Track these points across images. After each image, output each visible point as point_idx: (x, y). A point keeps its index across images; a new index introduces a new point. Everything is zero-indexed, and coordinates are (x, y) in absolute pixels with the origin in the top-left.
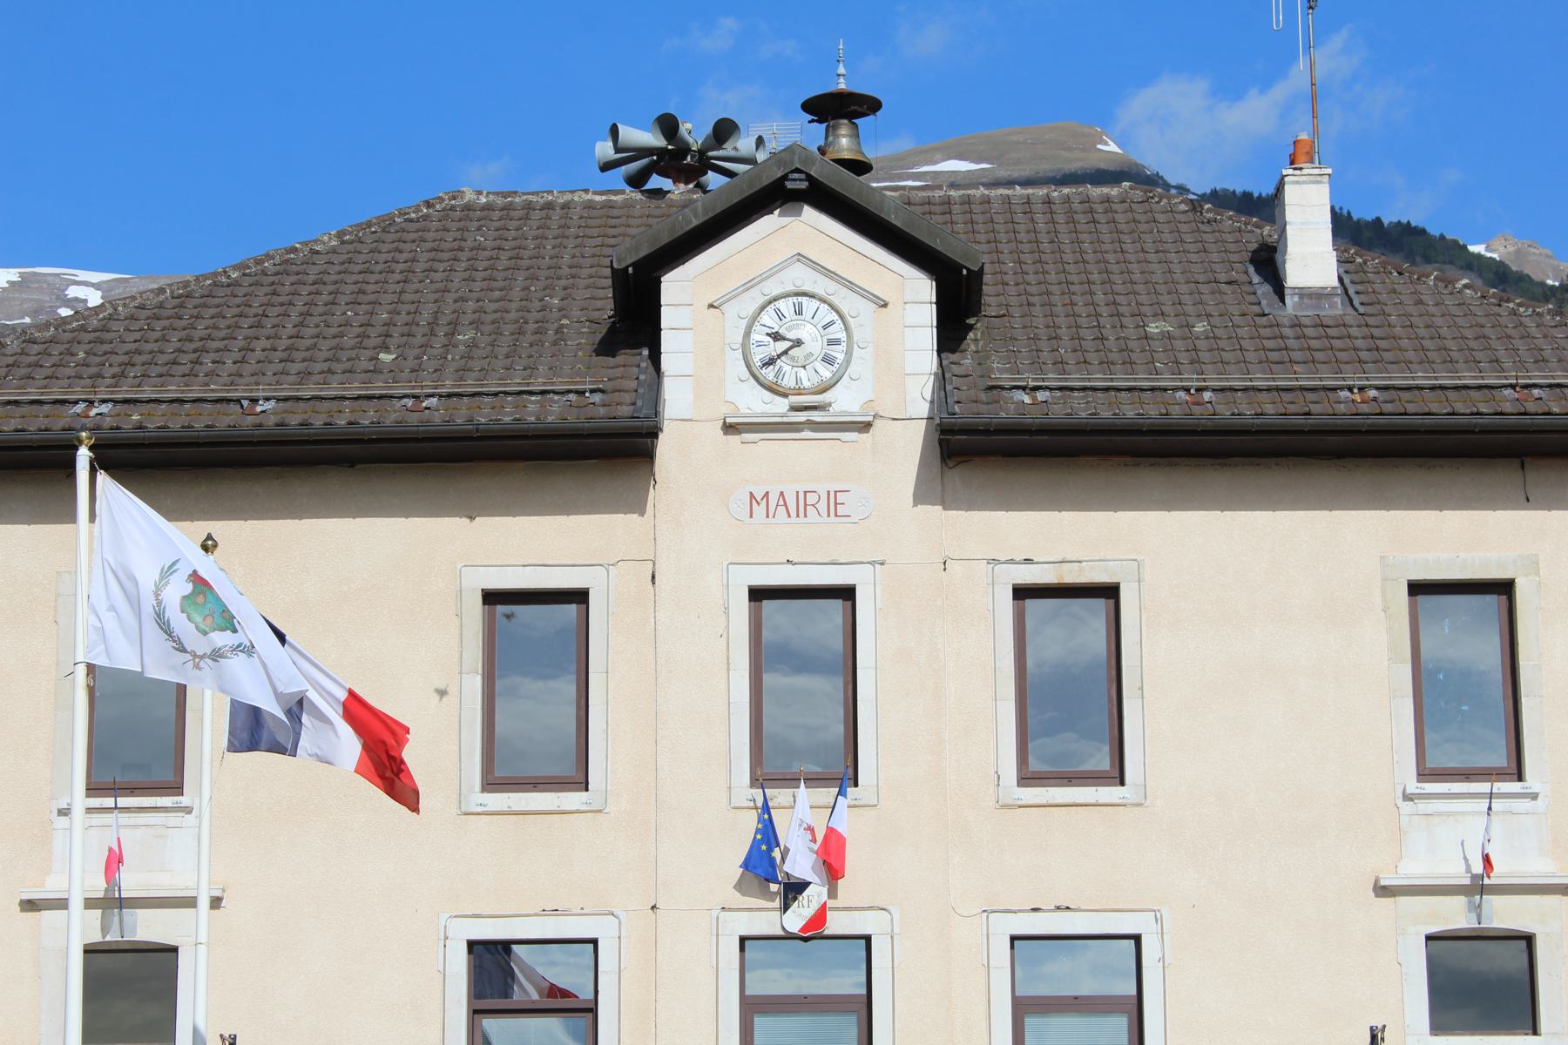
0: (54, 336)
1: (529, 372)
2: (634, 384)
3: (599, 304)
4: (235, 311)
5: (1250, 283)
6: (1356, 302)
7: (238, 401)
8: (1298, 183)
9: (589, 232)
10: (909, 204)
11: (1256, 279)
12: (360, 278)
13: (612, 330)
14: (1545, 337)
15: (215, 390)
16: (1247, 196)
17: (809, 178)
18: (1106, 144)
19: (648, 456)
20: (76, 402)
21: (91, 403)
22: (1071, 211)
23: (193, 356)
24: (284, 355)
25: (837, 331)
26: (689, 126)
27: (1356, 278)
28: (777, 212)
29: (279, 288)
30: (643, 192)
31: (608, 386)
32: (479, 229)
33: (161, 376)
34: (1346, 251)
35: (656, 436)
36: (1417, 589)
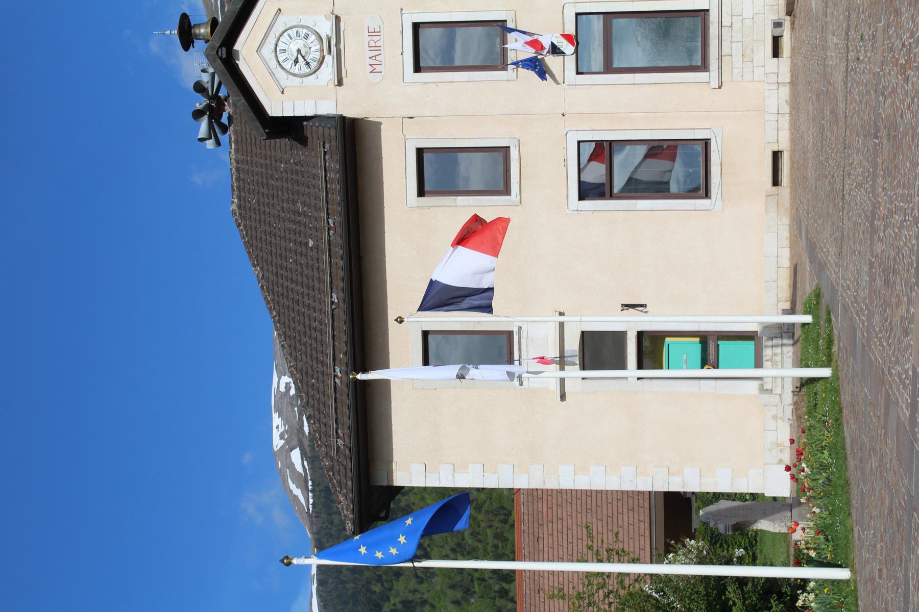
0: (305, 393)
1: (316, 177)
2: (320, 128)
3: (283, 145)
4: (291, 312)
7: (333, 310)
12: (274, 256)
13: (295, 139)
15: (328, 320)
17: (220, 47)
20: (335, 383)
21: (335, 376)
23: (313, 331)
25: (293, 32)
26: (197, 105)
28: (237, 62)
30: (229, 127)
31: (321, 140)
32: (249, 202)
33: (322, 345)
35: (344, 118)
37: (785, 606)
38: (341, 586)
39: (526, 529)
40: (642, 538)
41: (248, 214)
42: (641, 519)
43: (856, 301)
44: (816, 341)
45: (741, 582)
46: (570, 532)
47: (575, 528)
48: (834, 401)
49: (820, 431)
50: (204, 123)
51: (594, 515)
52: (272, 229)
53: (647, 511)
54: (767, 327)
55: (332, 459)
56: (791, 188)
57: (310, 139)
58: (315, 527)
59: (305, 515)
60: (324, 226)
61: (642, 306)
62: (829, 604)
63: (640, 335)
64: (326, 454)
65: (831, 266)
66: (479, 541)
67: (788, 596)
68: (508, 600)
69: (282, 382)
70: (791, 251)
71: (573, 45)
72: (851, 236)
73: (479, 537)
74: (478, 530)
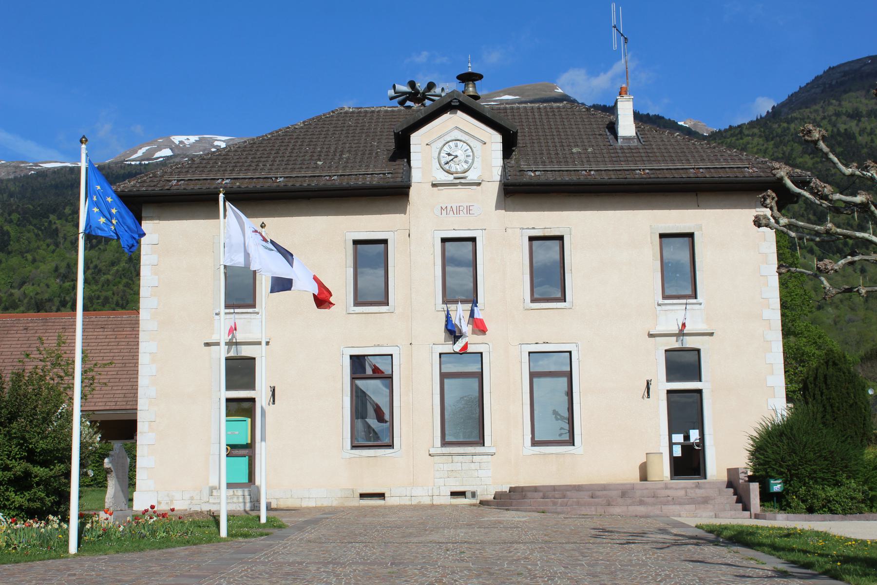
4: (270, 148)
5: (606, 135)
6: (642, 141)
7: (271, 178)
11: (608, 134)
12: (310, 136)
13: (394, 153)
16: (605, 106)
17: (459, 101)
20: (218, 179)
21: (223, 179)
22: (546, 112)
25: (469, 152)
26: (419, 84)
27: (642, 133)
31: (394, 172)
32: (350, 120)
33: (245, 170)
36: (662, 236)
39: (110, 319)
40: (104, 404)
41: (341, 119)
42: (118, 403)
44: (247, 526)
45: (68, 475)
46: (108, 351)
48: (202, 539)
49: (180, 530)
51: (121, 369)
53: (123, 407)
54: (258, 490)
55: (162, 176)
56: (359, 507)
57: (394, 163)
58: (114, 165)
59: (122, 158)
61: (274, 401)
64: (166, 172)
65: (301, 535)
66: (103, 286)
67: (58, 509)
68: (58, 306)
69: (221, 142)
70: (313, 507)
71: (460, 351)
73: (106, 285)
74: (111, 285)
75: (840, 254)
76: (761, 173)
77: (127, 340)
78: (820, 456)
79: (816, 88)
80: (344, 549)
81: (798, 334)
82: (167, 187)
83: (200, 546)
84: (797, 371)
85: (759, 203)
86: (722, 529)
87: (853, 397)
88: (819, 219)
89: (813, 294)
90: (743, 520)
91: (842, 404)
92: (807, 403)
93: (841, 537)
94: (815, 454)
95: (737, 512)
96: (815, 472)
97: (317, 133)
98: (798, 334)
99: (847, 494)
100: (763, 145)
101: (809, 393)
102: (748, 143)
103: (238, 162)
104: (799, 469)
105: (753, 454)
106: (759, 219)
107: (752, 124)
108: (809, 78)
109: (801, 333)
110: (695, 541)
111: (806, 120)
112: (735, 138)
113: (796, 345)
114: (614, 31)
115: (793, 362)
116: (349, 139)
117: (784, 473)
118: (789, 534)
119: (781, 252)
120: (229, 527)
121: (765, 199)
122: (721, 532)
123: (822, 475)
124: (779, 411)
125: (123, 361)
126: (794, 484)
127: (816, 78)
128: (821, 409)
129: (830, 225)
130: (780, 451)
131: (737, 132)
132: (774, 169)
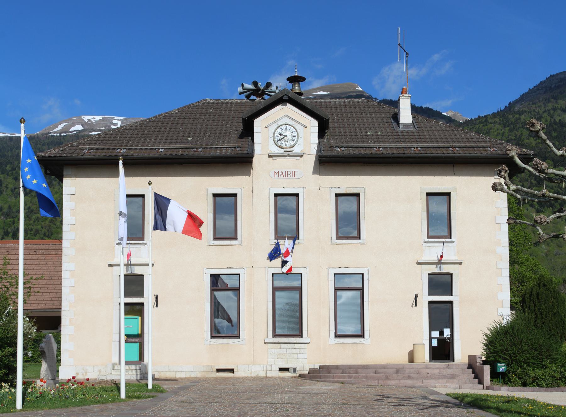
0: (112, 133)
1: (223, 143)
2: (247, 146)
3: (239, 126)
4: (154, 127)
5: (392, 122)
6: (416, 127)
7: (155, 149)
8: (403, 98)
9: (237, 109)
10: (312, 103)
11: (393, 121)
12: (183, 120)
13: (242, 133)
14: (460, 136)
15: (150, 146)
16: (391, 100)
17: (289, 97)
18: (358, 88)
19: (251, 163)
20: (118, 149)
21: (121, 149)
22: (350, 105)
23: (144, 138)
24: (166, 138)
25: (295, 133)
26: (260, 84)
27: (416, 121)
28: (281, 105)
29: (164, 122)
30: (250, 100)
31: (242, 146)
32: (211, 108)
33: (137, 143)
34: (414, 115)
35: (253, 158)
36: (428, 194)
37: (1, 377)
38: (9, 149)
39: (41, 246)
40: (37, 305)
41: (205, 107)
42: (47, 305)
43: (159, 410)
44: (139, 391)
45: (14, 355)
46: (40, 268)
47: (42, 271)
48: (108, 400)
49: (93, 393)
50: (251, 87)
51: (48, 281)
52: (197, 119)
53: (51, 307)
54: (146, 367)
55: (78, 146)
56: (216, 378)
57: (242, 140)
58: (41, 136)
59: (47, 131)
60: (198, 146)
61: (157, 305)
62: (3, 399)
63: (142, 304)
64: (80, 143)
65: (177, 398)
66: (34, 221)
67: (7, 378)
68: (3, 236)
69: (118, 122)
70: (184, 378)
71: (287, 272)
72: (191, 407)
73: (36, 221)
74: (40, 221)
75: (552, 208)
76: (499, 152)
77: (53, 260)
78: (533, 348)
79: (541, 90)
80: (207, 407)
81: (521, 263)
82: (81, 154)
83: (107, 405)
84: (519, 289)
85: (496, 173)
86: (464, 396)
87: (556, 308)
88: (539, 183)
89: (532, 235)
90: (478, 390)
91: (549, 313)
92: (524, 312)
93: (544, 403)
94: (529, 346)
95: (474, 385)
96: (528, 359)
97: (187, 117)
98: (521, 263)
99: (549, 374)
100: (502, 130)
101: (526, 305)
102: (491, 128)
103: (132, 137)
104: (517, 356)
105: (486, 345)
106: (496, 186)
107: (494, 115)
108: (535, 84)
109: (523, 263)
110: (445, 404)
111: (532, 113)
112: (482, 125)
113: (519, 271)
114: (399, 47)
115: (516, 282)
116: (211, 122)
117: (507, 359)
118: (510, 400)
119: (511, 206)
120: (127, 391)
121: (501, 172)
122: (463, 399)
123: (533, 361)
124: (505, 317)
125: (50, 275)
126: (513, 366)
127: (540, 82)
128: (534, 316)
129: (545, 191)
130: (505, 344)
131: (483, 120)
132: (508, 150)
